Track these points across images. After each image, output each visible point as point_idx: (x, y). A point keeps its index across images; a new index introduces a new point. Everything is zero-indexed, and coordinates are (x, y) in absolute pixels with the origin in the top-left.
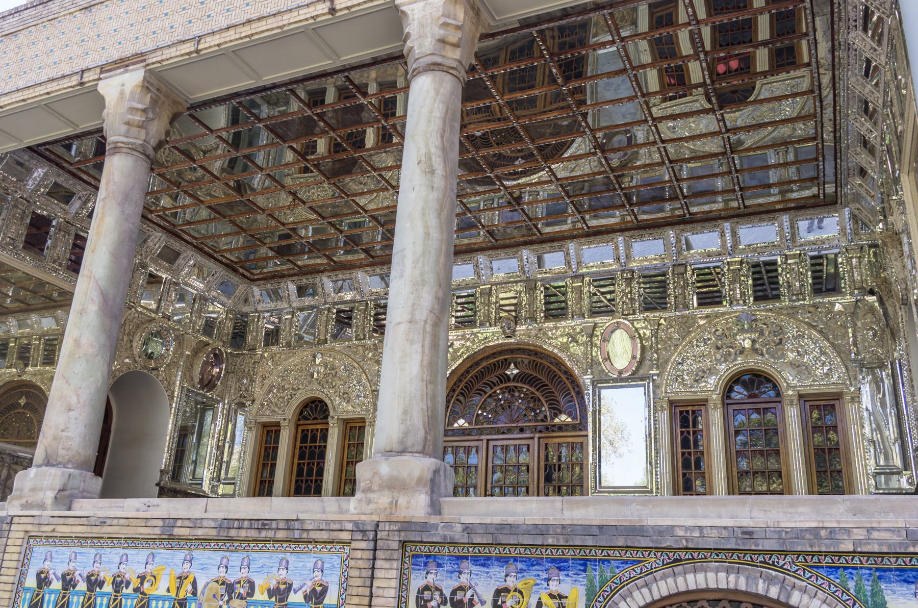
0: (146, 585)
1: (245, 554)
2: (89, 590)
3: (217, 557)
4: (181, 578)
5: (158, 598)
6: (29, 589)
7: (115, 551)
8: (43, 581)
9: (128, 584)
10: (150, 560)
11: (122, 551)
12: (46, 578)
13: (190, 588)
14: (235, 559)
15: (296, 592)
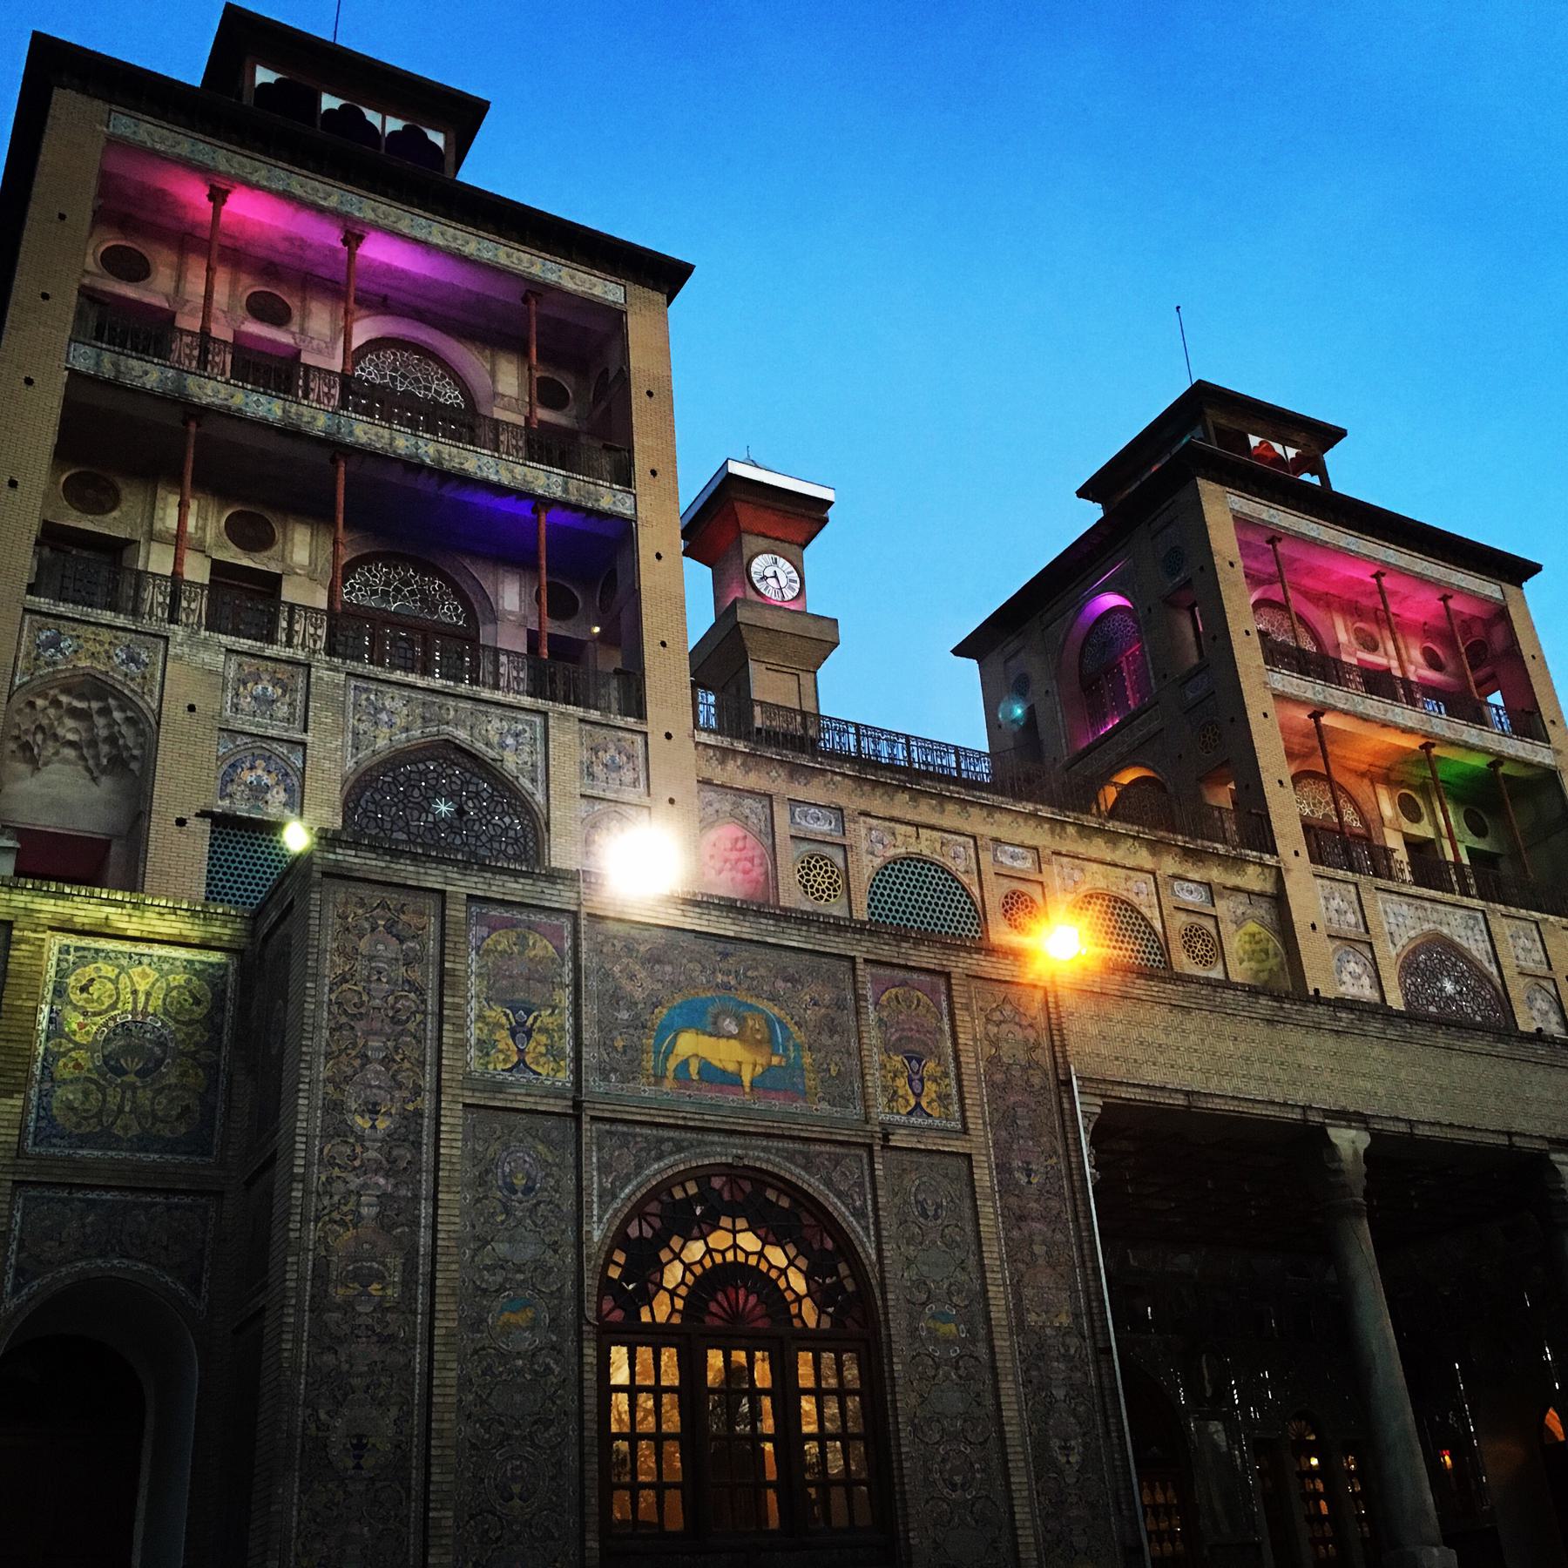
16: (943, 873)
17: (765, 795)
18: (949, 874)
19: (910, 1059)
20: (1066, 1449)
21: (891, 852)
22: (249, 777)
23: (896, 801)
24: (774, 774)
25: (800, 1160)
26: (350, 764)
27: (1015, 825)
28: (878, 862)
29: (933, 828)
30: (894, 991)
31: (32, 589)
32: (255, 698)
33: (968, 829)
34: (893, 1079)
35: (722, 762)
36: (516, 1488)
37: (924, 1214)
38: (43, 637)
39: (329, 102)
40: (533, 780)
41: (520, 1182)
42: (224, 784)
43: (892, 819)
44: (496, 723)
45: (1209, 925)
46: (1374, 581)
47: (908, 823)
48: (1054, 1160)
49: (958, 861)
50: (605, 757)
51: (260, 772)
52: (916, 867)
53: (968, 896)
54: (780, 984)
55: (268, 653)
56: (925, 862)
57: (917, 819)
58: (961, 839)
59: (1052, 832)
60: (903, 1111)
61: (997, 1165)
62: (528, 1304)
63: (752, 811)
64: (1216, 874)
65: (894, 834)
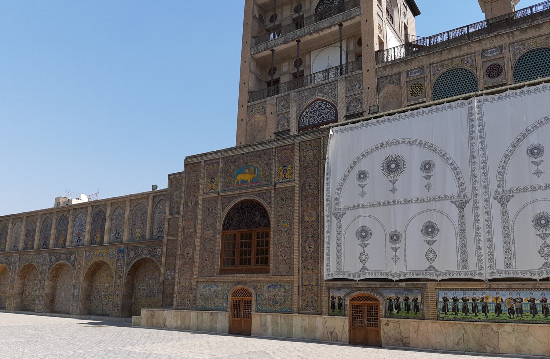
0: (484, 300)
1: (517, 292)
2: (464, 302)
3: (508, 293)
4: (497, 299)
5: (490, 303)
6: (441, 302)
7: (470, 292)
8: (445, 300)
9: (478, 300)
10: (484, 294)
11: (473, 292)
12: (446, 299)
13: (500, 300)
14: (514, 293)
15: (537, 300)
16: (462, 70)
18: (465, 69)
19: (284, 167)
20: (310, 247)
21: (442, 71)
22: (282, 123)
23: (443, 55)
25: (258, 195)
26: (298, 111)
27: (491, 41)
29: (458, 57)
31: (248, 102)
32: (282, 106)
33: (472, 51)
34: (280, 173)
35: (385, 70)
36: (207, 259)
40: (335, 98)
41: (211, 209)
43: (442, 61)
44: (327, 88)
47: (448, 60)
48: (317, 181)
53: (472, 74)
54: (258, 158)
55: (283, 95)
56: (455, 70)
57: (451, 57)
58: (469, 56)
59: (508, 37)
60: (281, 179)
61: (302, 186)
62: (210, 229)
63: (395, 79)
65: (443, 66)
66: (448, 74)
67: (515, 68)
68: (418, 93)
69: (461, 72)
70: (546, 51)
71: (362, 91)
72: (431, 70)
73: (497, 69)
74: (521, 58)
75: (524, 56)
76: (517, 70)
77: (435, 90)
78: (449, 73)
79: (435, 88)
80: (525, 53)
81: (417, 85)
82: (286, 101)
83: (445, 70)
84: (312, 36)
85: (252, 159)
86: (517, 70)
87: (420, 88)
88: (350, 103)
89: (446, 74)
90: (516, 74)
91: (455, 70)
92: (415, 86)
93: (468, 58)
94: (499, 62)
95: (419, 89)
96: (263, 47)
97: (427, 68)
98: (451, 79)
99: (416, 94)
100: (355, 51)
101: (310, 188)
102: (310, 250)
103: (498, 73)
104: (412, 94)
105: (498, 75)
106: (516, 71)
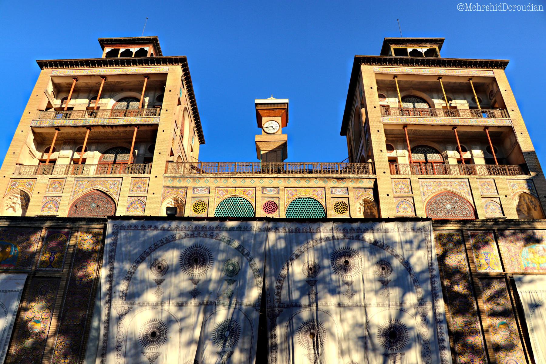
17: (185, 187)
18: (246, 199)
22: (49, 206)
24: (188, 181)
26: (72, 199)
27: (271, 182)
28: (220, 200)
30: (54, 235)
35: (173, 181)
37: (42, 293)
38: (13, 184)
39: (122, 50)
42: (43, 208)
44: (110, 182)
45: (346, 201)
46: (438, 81)
49: (249, 195)
50: (137, 186)
51: (51, 204)
52: (234, 199)
53: (251, 205)
56: (237, 197)
57: (236, 186)
59: (285, 181)
60: (45, 267)
61: (71, 280)
64: (349, 184)
66: (230, 200)
67: (288, 209)
68: (201, 211)
69: (242, 201)
70: (312, 201)
71: (146, 195)
72: (216, 193)
73: (272, 206)
74: (293, 202)
75: (295, 201)
76: (289, 212)
77: (217, 212)
78: (231, 199)
79: (217, 209)
80: (297, 199)
81: (201, 203)
82: (60, 183)
83: (229, 195)
84: (105, 128)
85: (11, 235)
86: (289, 212)
87: (204, 206)
88: (131, 204)
89: (229, 199)
90: (288, 215)
91: (235, 197)
92: (199, 203)
93: (249, 190)
94: (276, 200)
95: (202, 207)
96: (47, 123)
97: (213, 190)
98: (233, 205)
99: (199, 211)
100: (144, 155)
101: (80, 284)
102: (64, 362)
103: (273, 210)
104: (195, 210)
105: (273, 212)
106: (288, 212)
